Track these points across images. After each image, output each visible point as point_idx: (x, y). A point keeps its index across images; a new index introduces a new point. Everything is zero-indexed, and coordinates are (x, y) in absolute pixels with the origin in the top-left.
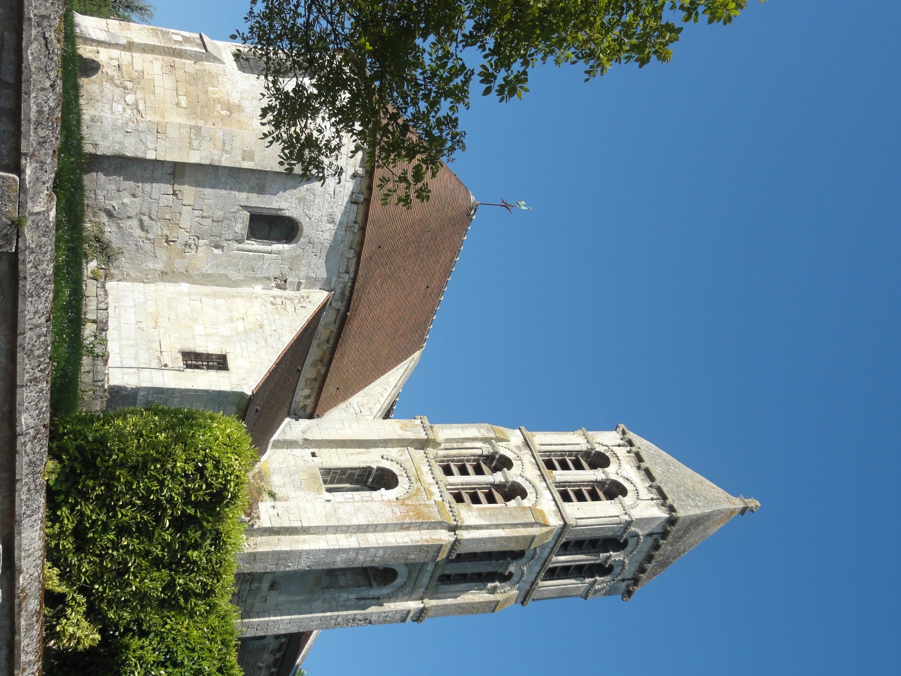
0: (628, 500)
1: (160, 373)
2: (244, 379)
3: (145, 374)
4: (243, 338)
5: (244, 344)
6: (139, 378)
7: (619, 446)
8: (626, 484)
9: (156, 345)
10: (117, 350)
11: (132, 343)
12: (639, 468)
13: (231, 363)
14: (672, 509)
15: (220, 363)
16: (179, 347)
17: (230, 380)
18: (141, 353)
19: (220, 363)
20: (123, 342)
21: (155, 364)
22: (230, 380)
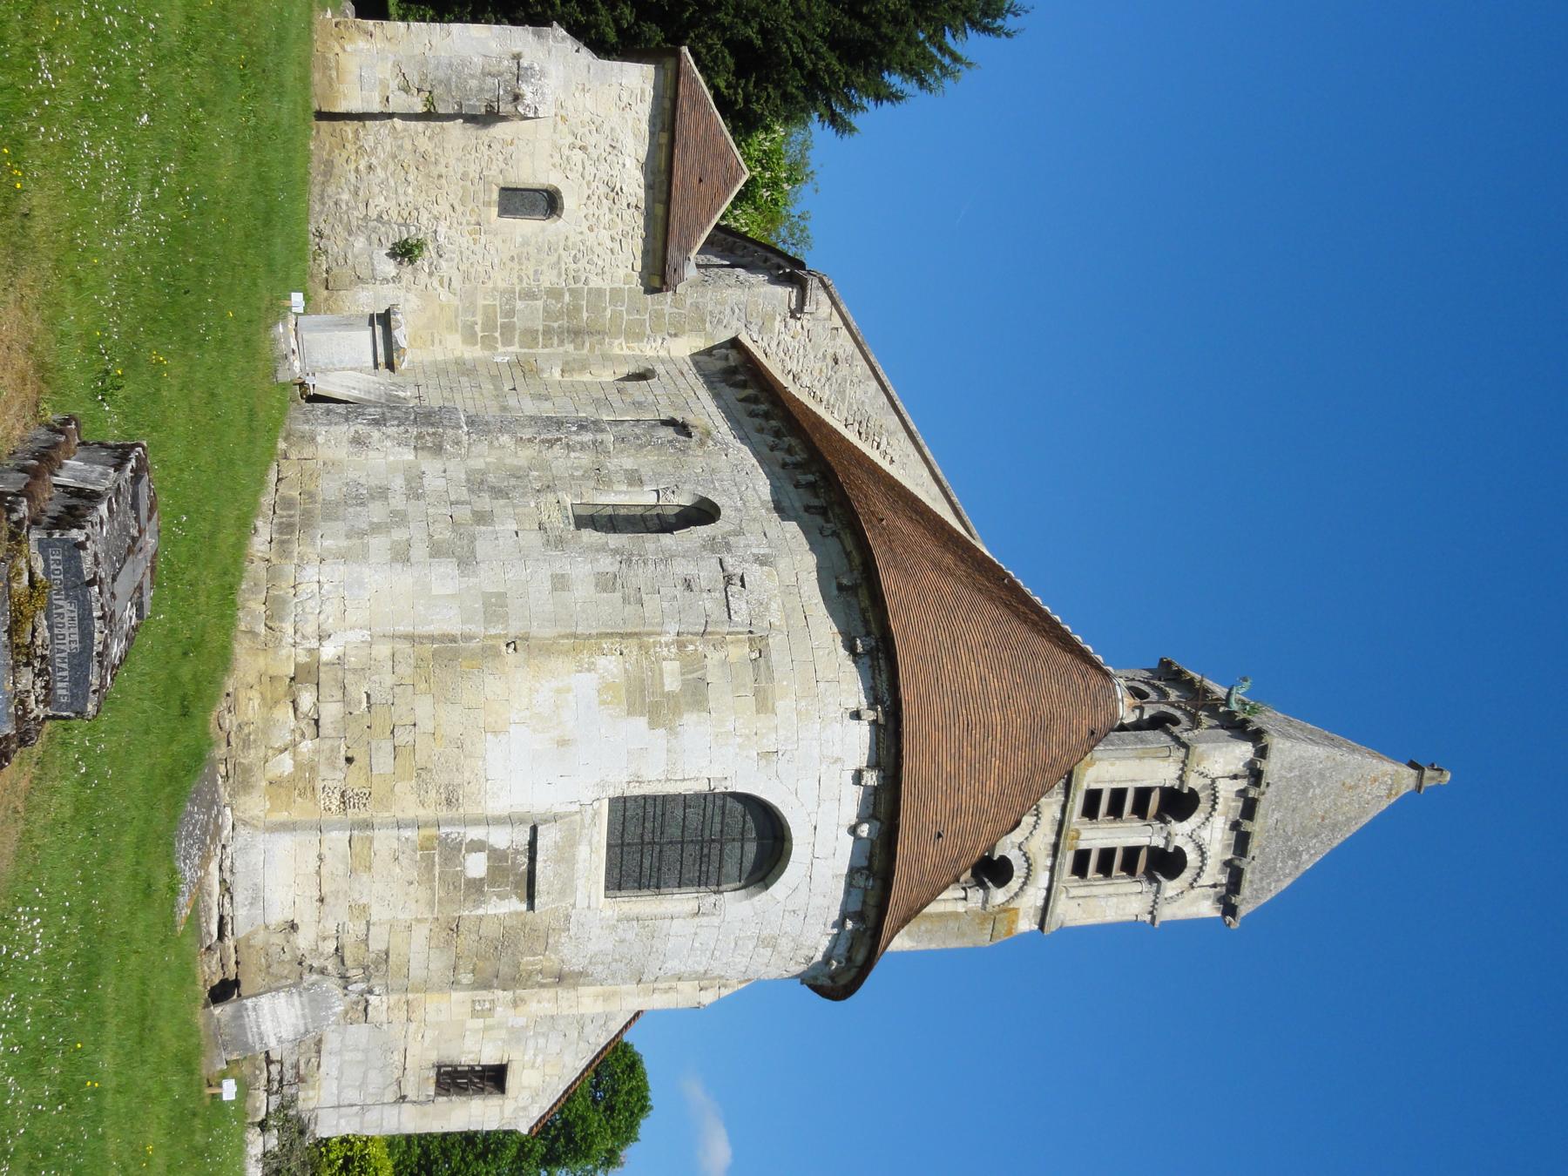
0: (1170, 887)
1: (395, 1110)
2: (524, 1109)
3: (373, 1116)
4: (545, 1029)
5: (542, 1041)
6: (362, 1123)
7: (1235, 777)
8: (1192, 857)
9: (397, 1057)
10: (334, 1073)
11: (360, 1056)
12: (1235, 826)
13: (511, 1081)
14: (1229, 909)
15: (494, 1078)
16: (434, 1057)
17: (502, 1112)
18: (374, 1076)
19: (494, 1078)
20: (348, 1056)
21: (390, 1096)
22: (502, 1112)
